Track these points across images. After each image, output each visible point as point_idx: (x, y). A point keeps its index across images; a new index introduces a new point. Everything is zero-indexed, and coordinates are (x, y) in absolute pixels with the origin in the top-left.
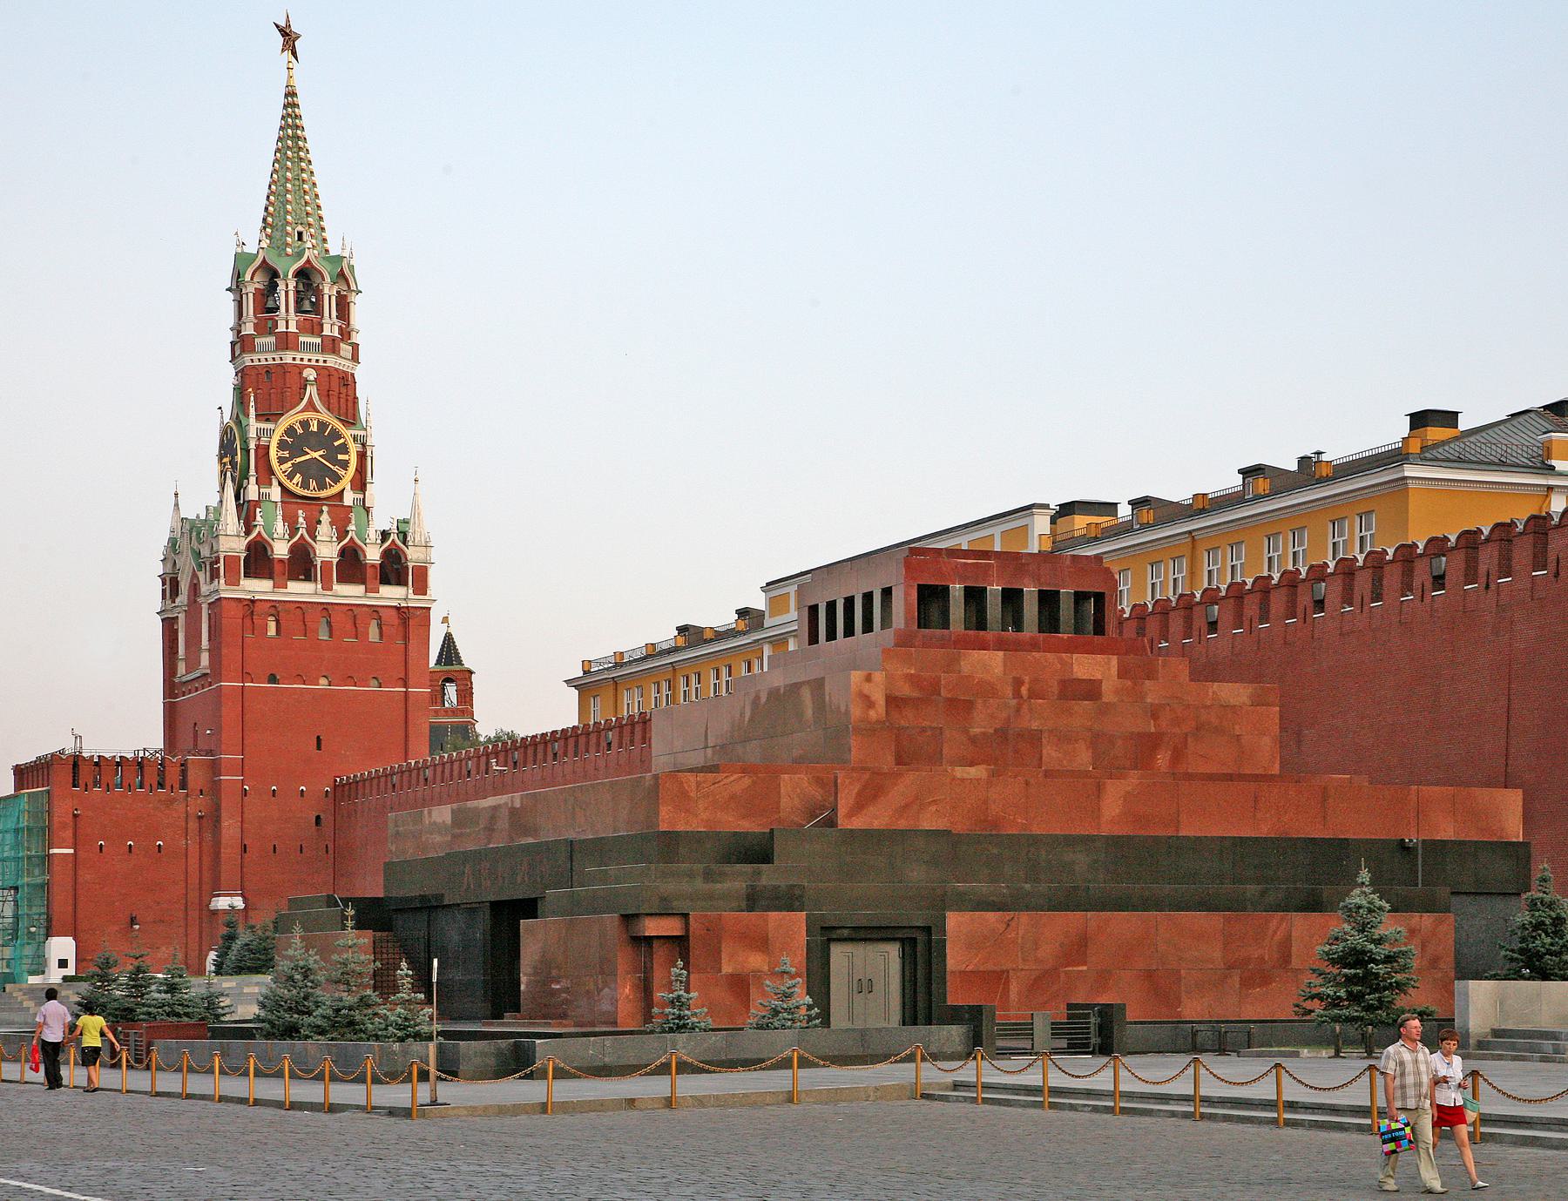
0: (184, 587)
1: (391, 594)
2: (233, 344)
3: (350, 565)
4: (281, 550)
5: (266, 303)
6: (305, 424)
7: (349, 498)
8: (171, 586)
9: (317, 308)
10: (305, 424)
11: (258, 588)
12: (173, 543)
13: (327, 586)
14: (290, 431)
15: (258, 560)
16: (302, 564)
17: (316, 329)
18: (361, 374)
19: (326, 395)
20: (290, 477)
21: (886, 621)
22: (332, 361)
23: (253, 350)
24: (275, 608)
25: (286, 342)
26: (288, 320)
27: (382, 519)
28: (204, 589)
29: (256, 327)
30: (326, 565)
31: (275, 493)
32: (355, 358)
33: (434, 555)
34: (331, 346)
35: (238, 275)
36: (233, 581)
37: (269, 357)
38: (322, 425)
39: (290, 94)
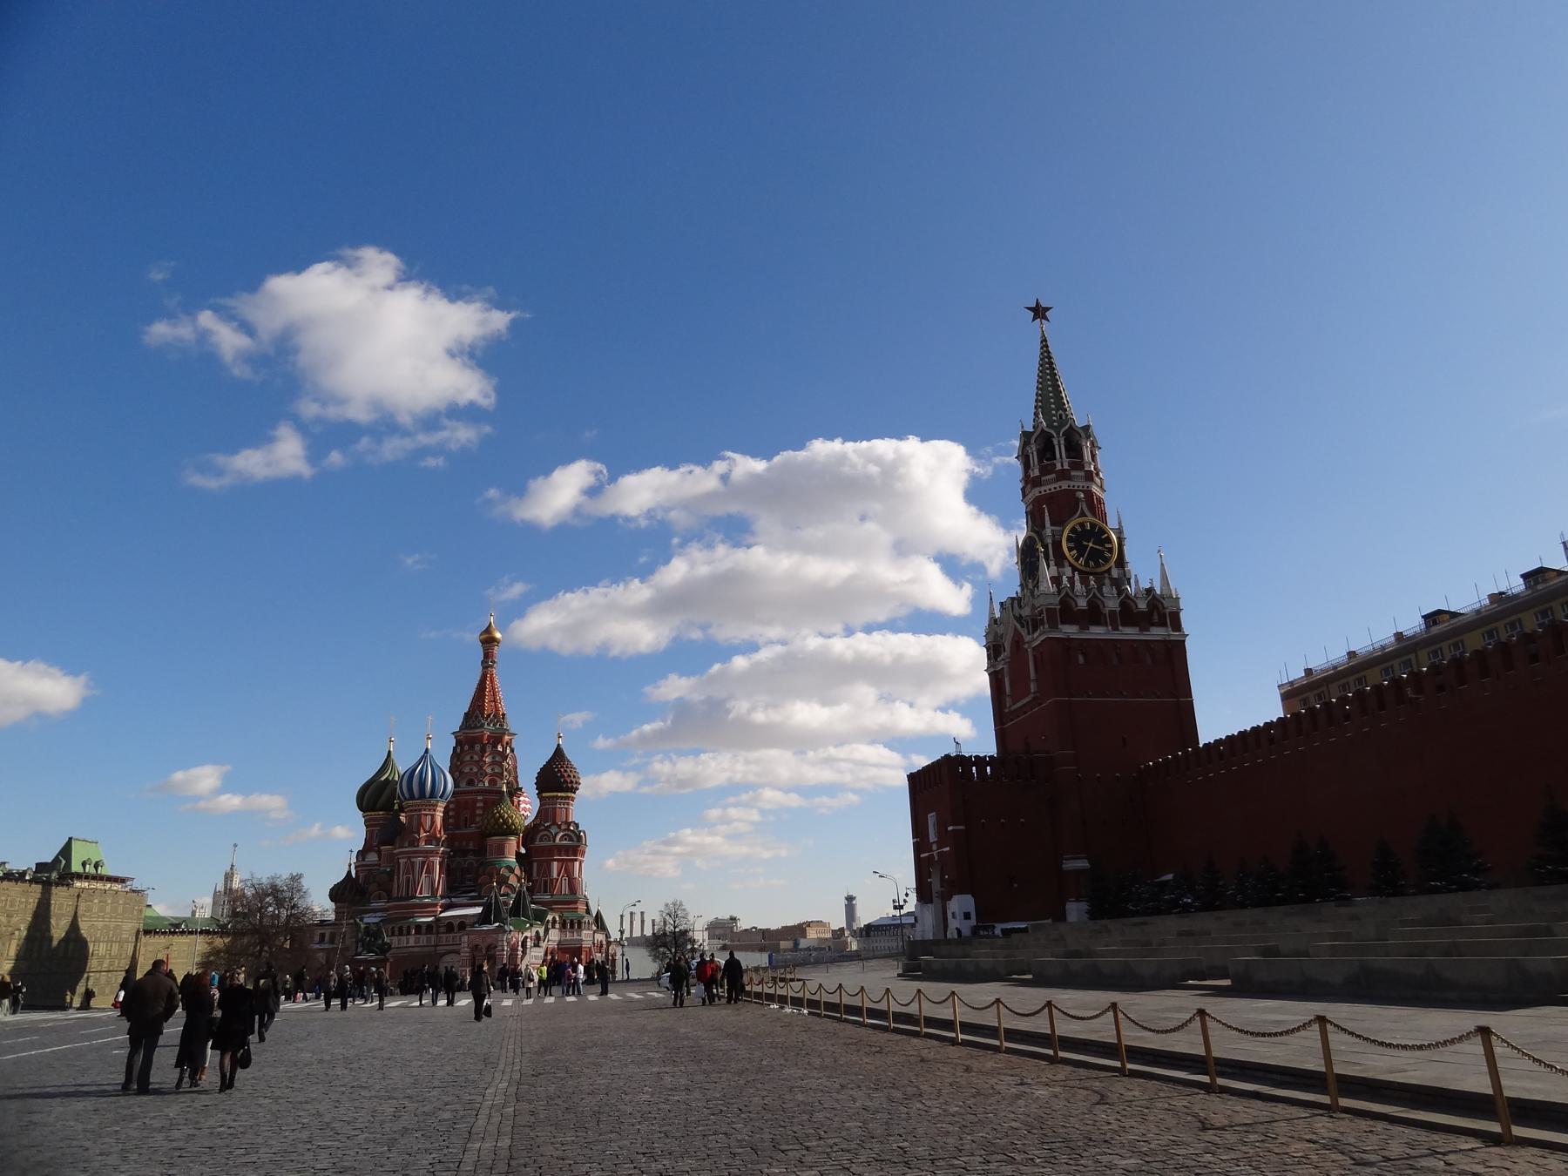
1: (1157, 633)
2: (1023, 489)
4: (1082, 603)
5: (1046, 450)
6: (1082, 525)
7: (1115, 573)
10: (1082, 525)
14: (1073, 530)
15: (1066, 612)
16: (1094, 615)
20: (1077, 560)
23: (1041, 485)
26: (1062, 461)
28: (1028, 638)
30: (1112, 613)
31: (1068, 571)
36: (1054, 626)
39: (1044, 340)
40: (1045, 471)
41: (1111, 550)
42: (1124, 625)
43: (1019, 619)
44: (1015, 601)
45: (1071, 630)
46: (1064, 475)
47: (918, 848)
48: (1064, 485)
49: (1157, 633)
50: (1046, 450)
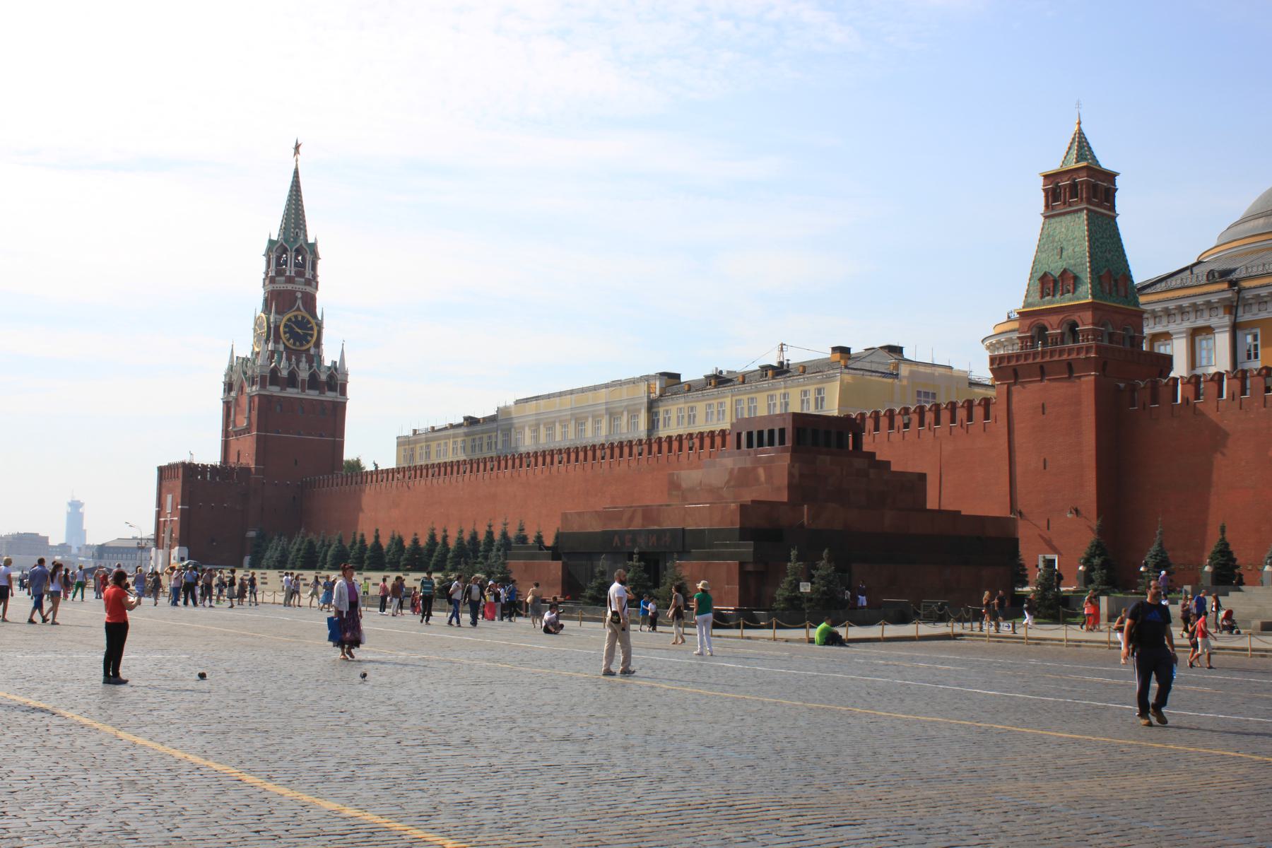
0: (236, 387)
1: (330, 396)
3: (314, 382)
4: (285, 373)
7: (312, 351)
8: (229, 387)
9: (303, 265)
10: (296, 317)
12: (231, 368)
13: (303, 391)
14: (289, 320)
16: (292, 380)
18: (318, 295)
19: (305, 304)
21: (782, 442)
22: (308, 289)
25: (290, 280)
27: (327, 363)
30: (303, 381)
31: (281, 347)
32: (317, 288)
38: (303, 318)
39: (296, 173)
40: (279, 273)
41: (312, 336)
42: (310, 388)
45: (274, 390)
46: (290, 280)
47: (159, 514)
48: (290, 287)
49: (330, 396)
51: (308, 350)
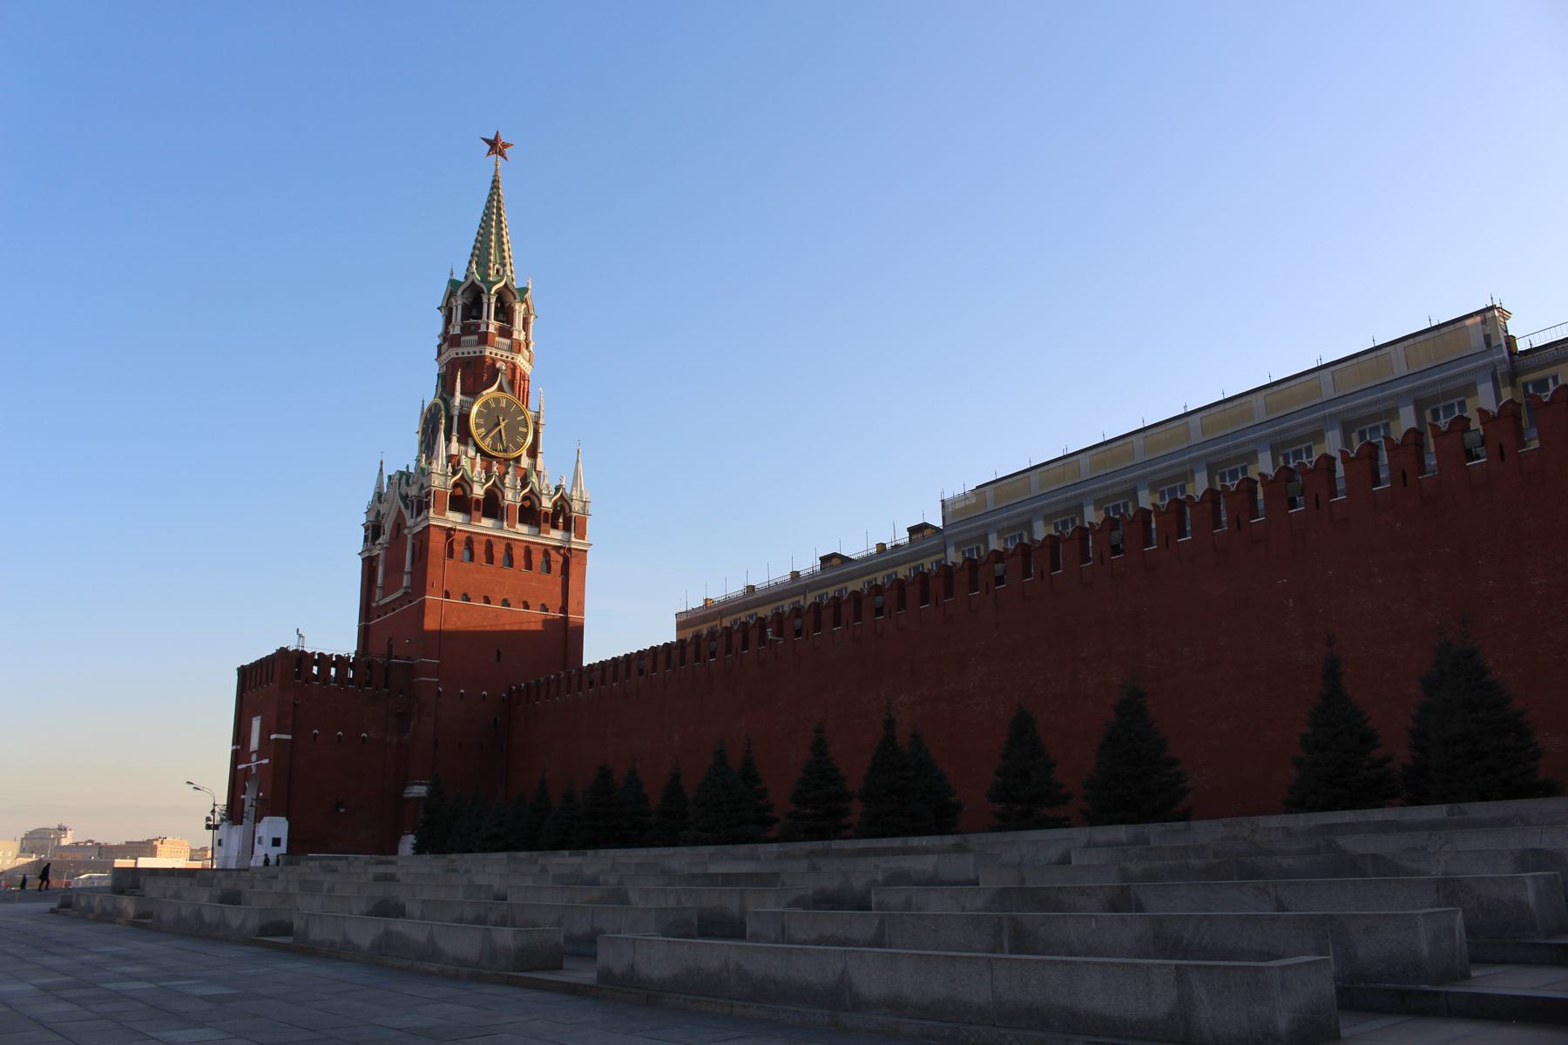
0: (388, 526)
1: (555, 536)
2: (440, 347)
7: (525, 462)
8: (373, 531)
10: (497, 400)
11: (454, 519)
12: (379, 496)
14: (486, 405)
17: (506, 333)
19: (512, 383)
24: (470, 542)
28: (410, 522)
29: (462, 329)
33: (590, 508)
34: (515, 348)
35: (451, 295)
37: (471, 350)
42: (522, 521)
43: (404, 498)
44: (404, 476)
47: (236, 757)
50: (474, 307)
51: (518, 460)
